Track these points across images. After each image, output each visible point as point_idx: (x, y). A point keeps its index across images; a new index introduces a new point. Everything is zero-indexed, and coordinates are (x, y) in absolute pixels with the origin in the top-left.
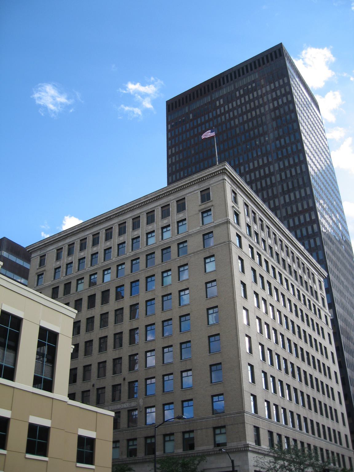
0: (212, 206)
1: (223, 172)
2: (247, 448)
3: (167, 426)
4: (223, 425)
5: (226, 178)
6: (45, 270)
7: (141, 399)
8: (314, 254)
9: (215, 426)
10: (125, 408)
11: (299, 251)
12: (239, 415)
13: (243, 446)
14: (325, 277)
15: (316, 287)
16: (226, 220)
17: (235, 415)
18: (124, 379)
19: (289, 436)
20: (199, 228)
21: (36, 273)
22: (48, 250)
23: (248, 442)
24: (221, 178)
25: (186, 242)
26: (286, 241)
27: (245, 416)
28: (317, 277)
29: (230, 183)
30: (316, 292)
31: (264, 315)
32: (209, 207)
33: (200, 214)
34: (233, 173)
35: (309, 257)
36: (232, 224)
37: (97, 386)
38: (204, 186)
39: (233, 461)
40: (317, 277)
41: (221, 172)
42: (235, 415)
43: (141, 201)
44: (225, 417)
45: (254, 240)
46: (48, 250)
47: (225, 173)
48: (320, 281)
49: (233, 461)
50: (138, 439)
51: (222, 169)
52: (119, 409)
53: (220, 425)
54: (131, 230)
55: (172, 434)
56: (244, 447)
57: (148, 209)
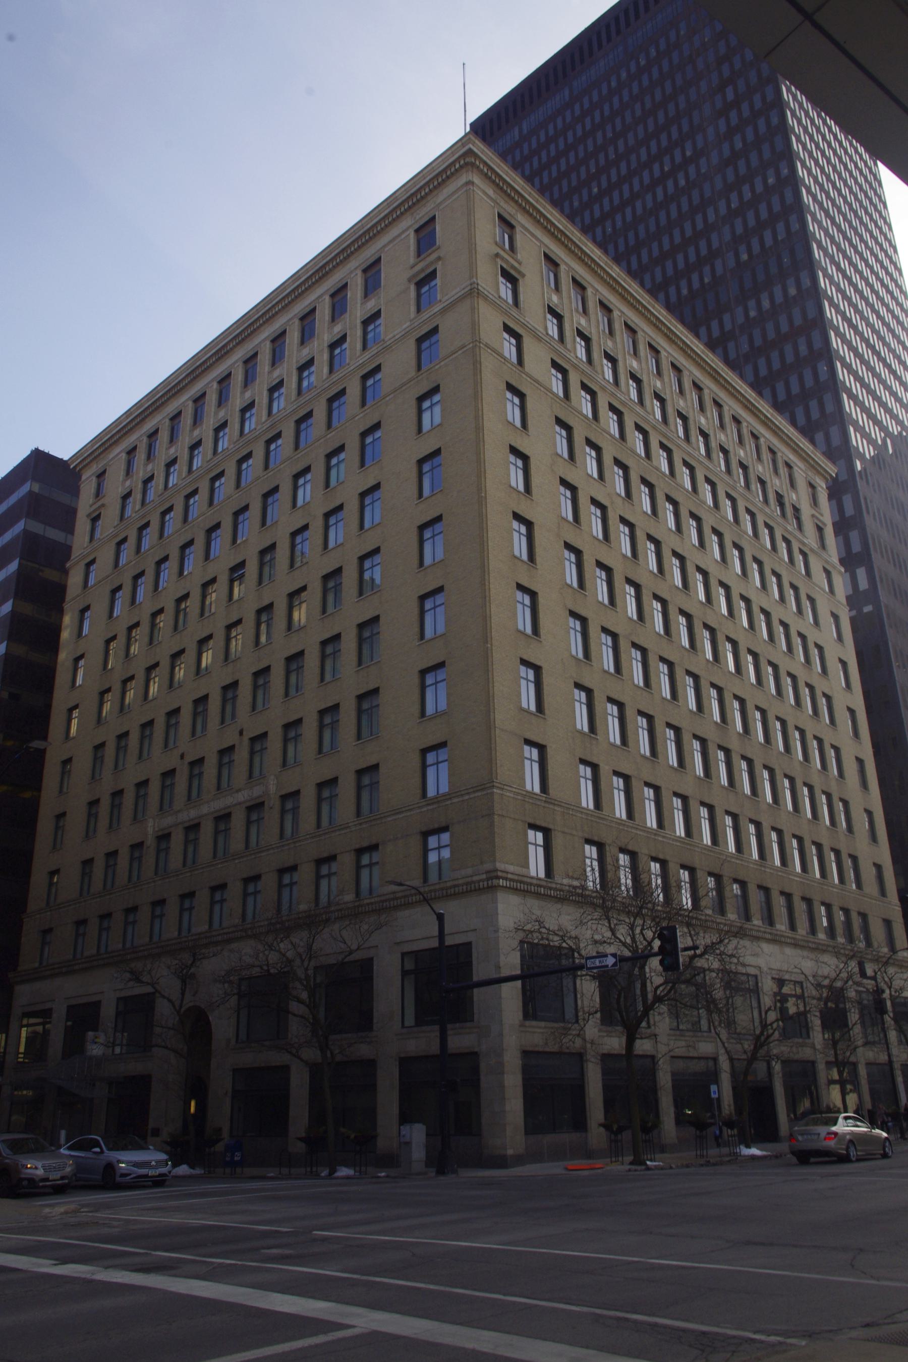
0: (439, 258)
1: (466, 164)
2: (495, 882)
3: (323, 838)
4: (444, 824)
5: (477, 180)
6: (103, 505)
7: (272, 777)
8: (767, 391)
9: (424, 829)
10: (240, 804)
11: (741, 402)
12: (479, 794)
13: (484, 876)
14: (831, 475)
15: (800, 497)
16: (469, 288)
17: (472, 796)
18: (241, 733)
19: (668, 858)
20: (408, 324)
21: (88, 516)
22: (111, 456)
23: (500, 866)
24: (463, 179)
25: (378, 369)
26: (625, 309)
27: (496, 797)
28: (801, 472)
29: (493, 196)
30: (796, 510)
31: (523, 498)
32: (432, 263)
33: (413, 288)
34: (499, 166)
35: (776, 419)
36: (486, 298)
37: (189, 758)
38: (421, 215)
39: (440, 918)
40: (801, 472)
41: (462, 162)
42: (472, 796)
43: (285, 289)
44: (449, 802)
45: (674, 430)
46: (111, 456)
47: (473, 165)
48: (812, 486)
49: (440, 918)
50: (263, 877)
51: (464, 155)
52: (229, 807)
53: (436, 826)
54: (267, 368)
55: (332, 858)
56: (488, 879)
57: (303, 306)
